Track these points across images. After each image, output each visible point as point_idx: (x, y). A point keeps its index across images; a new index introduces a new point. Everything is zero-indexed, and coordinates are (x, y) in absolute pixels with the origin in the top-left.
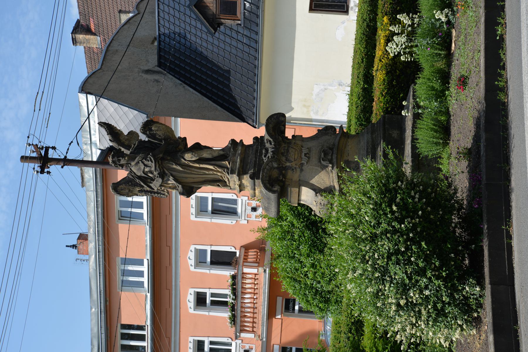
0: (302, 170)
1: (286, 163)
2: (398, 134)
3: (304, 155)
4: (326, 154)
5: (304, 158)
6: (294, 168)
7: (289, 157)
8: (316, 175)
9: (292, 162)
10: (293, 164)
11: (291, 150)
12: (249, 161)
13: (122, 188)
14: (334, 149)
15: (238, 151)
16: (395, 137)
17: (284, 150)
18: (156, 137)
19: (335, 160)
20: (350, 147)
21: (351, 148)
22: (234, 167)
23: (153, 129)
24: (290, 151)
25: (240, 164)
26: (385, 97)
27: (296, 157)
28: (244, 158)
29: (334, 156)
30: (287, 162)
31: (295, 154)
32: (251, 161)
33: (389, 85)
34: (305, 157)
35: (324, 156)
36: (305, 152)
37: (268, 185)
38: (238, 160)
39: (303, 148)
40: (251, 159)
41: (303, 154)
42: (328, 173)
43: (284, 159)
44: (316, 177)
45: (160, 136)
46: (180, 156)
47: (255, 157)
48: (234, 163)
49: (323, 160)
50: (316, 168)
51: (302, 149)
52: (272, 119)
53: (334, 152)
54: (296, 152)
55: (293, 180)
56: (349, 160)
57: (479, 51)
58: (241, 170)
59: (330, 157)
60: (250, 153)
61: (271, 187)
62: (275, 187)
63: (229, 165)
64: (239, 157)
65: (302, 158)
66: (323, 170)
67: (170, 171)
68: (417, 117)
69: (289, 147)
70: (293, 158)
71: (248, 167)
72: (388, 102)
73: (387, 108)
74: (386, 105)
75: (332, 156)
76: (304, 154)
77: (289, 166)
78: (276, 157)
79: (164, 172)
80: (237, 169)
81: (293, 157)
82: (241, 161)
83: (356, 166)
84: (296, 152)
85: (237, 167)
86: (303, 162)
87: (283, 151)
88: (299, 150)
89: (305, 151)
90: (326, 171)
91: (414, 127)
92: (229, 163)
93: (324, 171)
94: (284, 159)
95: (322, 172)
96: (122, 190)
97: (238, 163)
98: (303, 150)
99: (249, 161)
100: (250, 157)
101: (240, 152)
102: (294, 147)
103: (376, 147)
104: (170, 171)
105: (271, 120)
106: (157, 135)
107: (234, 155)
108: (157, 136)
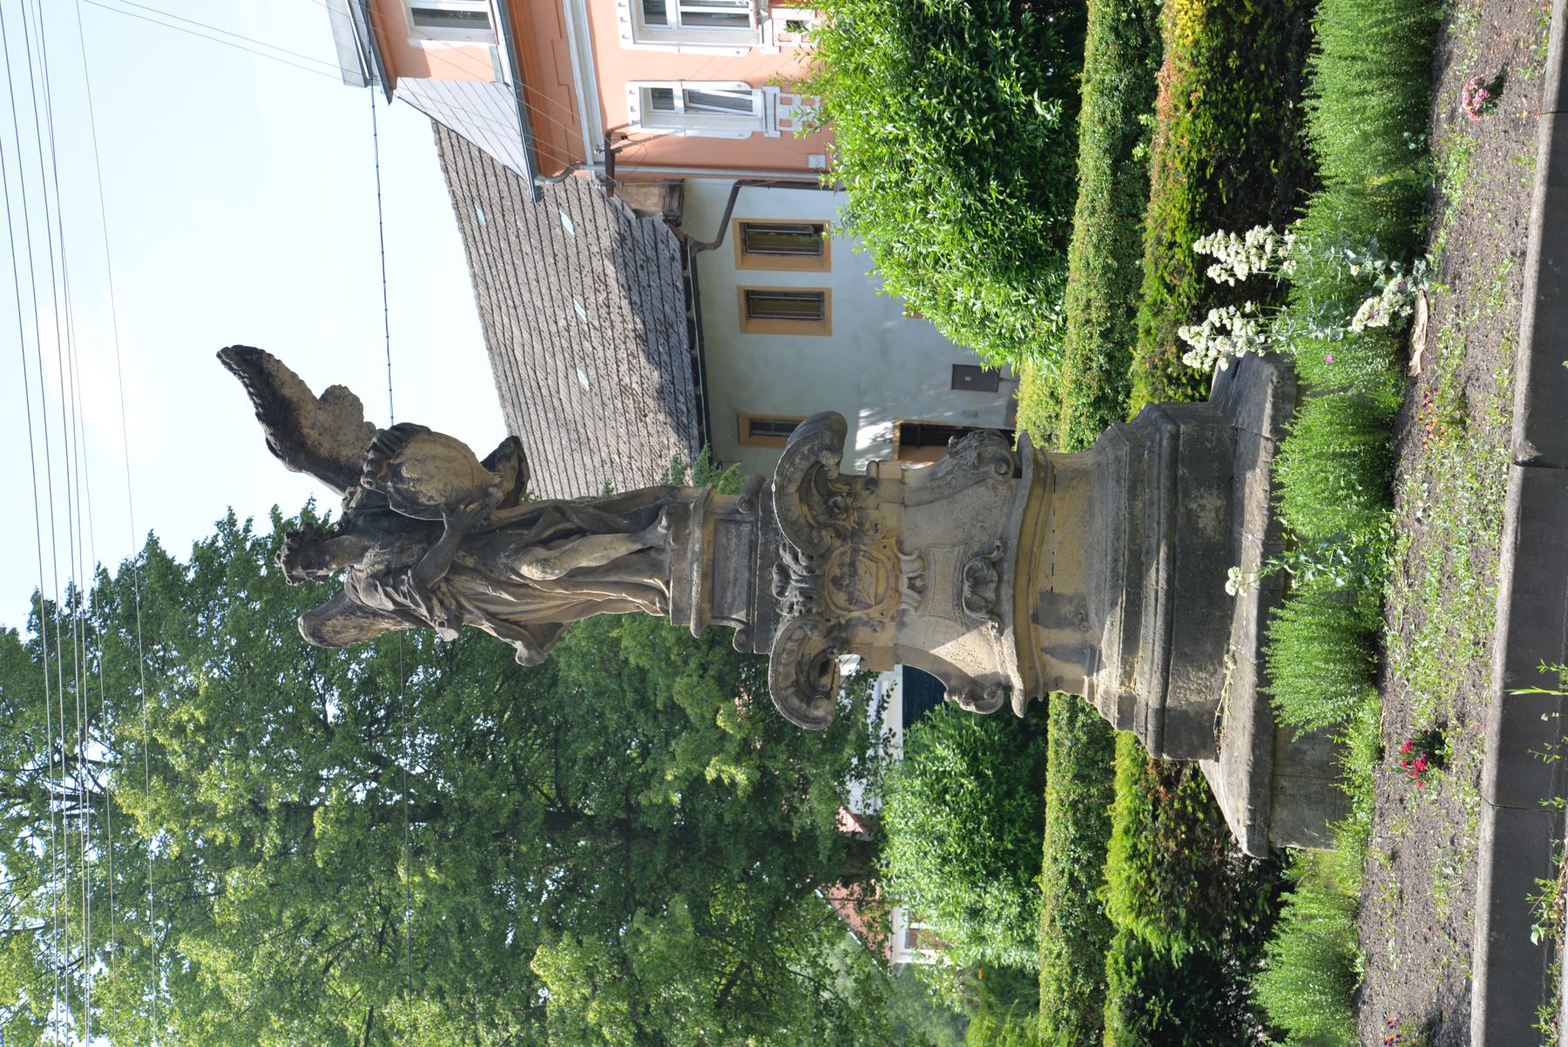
0: (902, 625)
1: (850, 611)
2: (1217, 510)
3: (906, 585)
4: (977, 582)
5: (907, 595)
6: (875, 623)
7: (857, 593)
8: (949, 641)
9: (870, 607)
10: (874, 612)
11: (863, 565)
12: (731, 575)
13: (334, 626)
14: (1006, 565)
15: (690, 546)
16: (1210, 528)
17: (841, 565)
18: (419, 504)
19: (1006, 607)
20: (1058, 536)
21: (1061, 543)
22: (685, 599)
23: (405, 473)
24: (861, 569)
25: (702, 593)
26: (1196, 116)
27: (881, 590)
28: (714, 560)
29: (1006, 593)
30: (853, 607)
31: (877, 579)
32: (736, 579)
33: (1212, 69)
34: (910, 592)
35: (973, 592)
36: (911, 575)
37: (796, 702)
38: (695, 576)
39: (902, 557)
40: (736, 571)
41: (904, 582)
42: (988, 641)
43: (841, 598)
44: (948, 645)
45: (431, 498)
46: (506, 565)
47: (750, 569)
48: (683, 582)
49: (968, 607)
50: (947, 622)
51: (899, 560)
52: (797, 460)
53: (1005, 578)
54: (882, 571)
55: (875, 644)
56: (1056, 591)
57: (1523, 254)
58: (707, 606)
59: (990, 595)
60: (733, 546)
61: (804, 706)
62: (817, 708)
63: (668, 588)
64: (695, 567)
65: (900, 594)
66: (968, 630)
67: (479, 604)
68: (1274, 592)
69: (855, 551)
70: (872, 595)
71: (729, 594)
72: (1205, 141)
73: (1203, 164)
74: (1199, 152)
75: (997, 590)
76: (906, 581)
77: (859, 619)
78: (814, 610)
79: (460, 606)
80: (693, 610)
81: (872, 591)
82: (704, 577)
83: (1077, 613)
84: (882, 571)
85: (694, 601)
86: (904, 606)
87: (837, 572)
88: (889, 566)
89: (909, 566)
90: (981, 633)
91: (1263, 619)
92: (667, 584)
93: (975, 632)
94: (841, 598)
95: (967, 636)
96: (339, 633)
97: (694, 589)
98: (905, 567)
99: (731, 575)
100: (733, 563)
101: (697, 547)
102: (875, 554)
103: (1143, 558)
104: (479, 604)
105: (792, 464)
106: (421, 495)
107: (681, 554)
108: (423, 500)
